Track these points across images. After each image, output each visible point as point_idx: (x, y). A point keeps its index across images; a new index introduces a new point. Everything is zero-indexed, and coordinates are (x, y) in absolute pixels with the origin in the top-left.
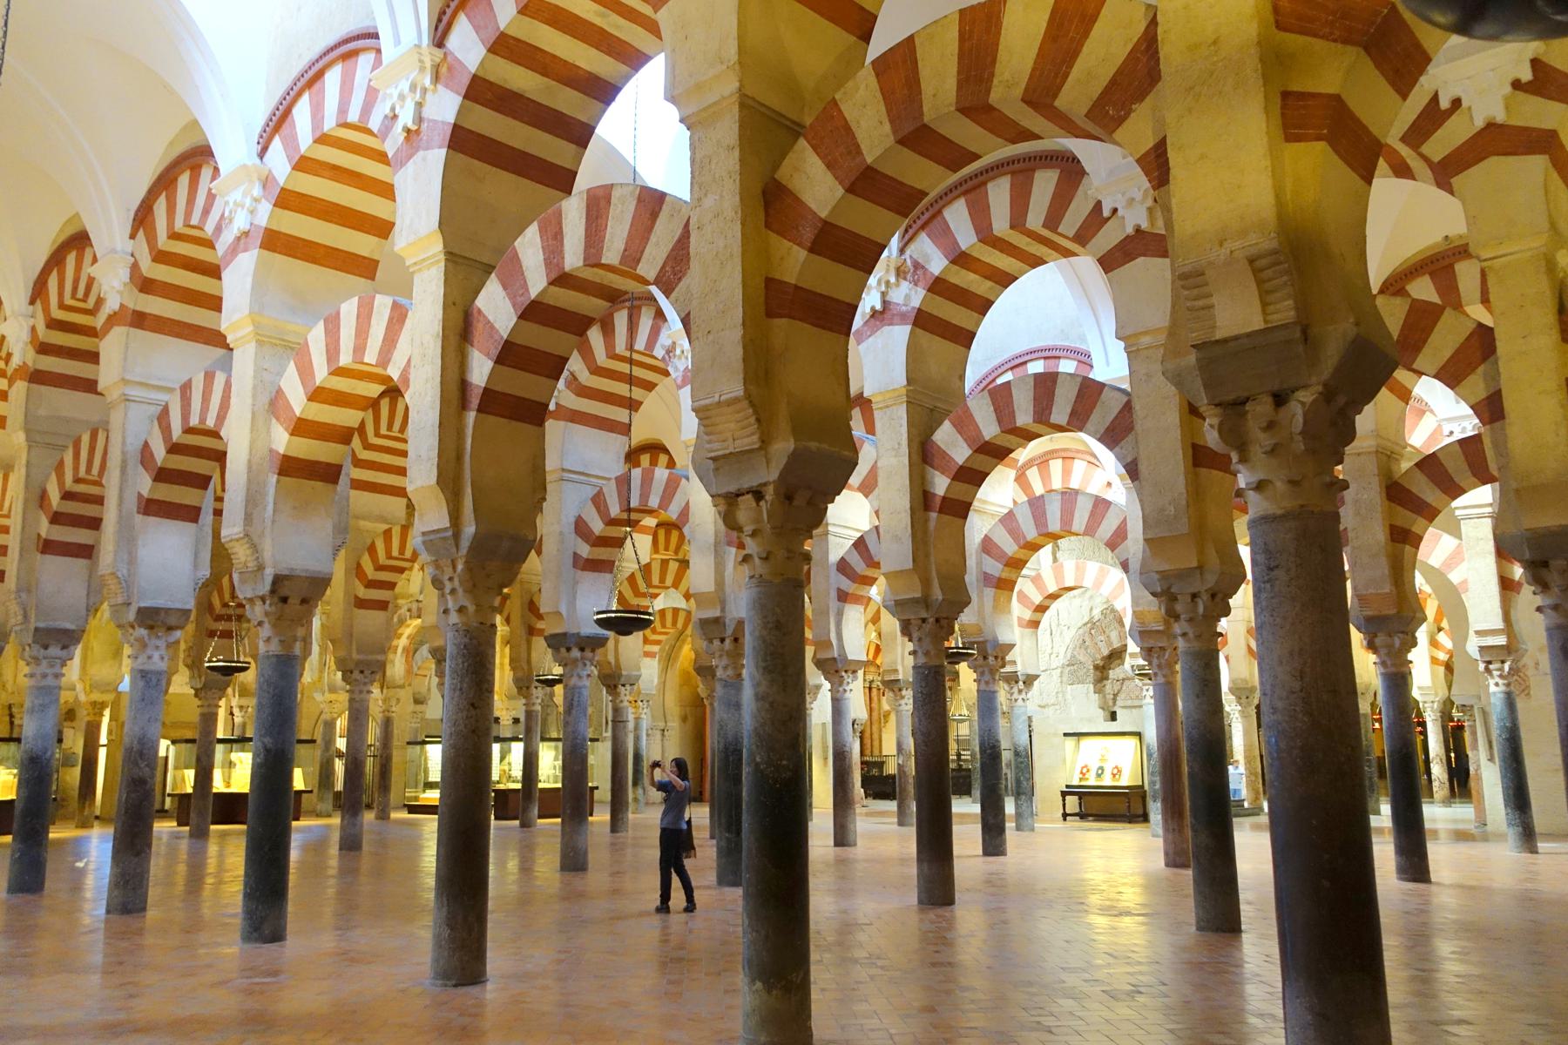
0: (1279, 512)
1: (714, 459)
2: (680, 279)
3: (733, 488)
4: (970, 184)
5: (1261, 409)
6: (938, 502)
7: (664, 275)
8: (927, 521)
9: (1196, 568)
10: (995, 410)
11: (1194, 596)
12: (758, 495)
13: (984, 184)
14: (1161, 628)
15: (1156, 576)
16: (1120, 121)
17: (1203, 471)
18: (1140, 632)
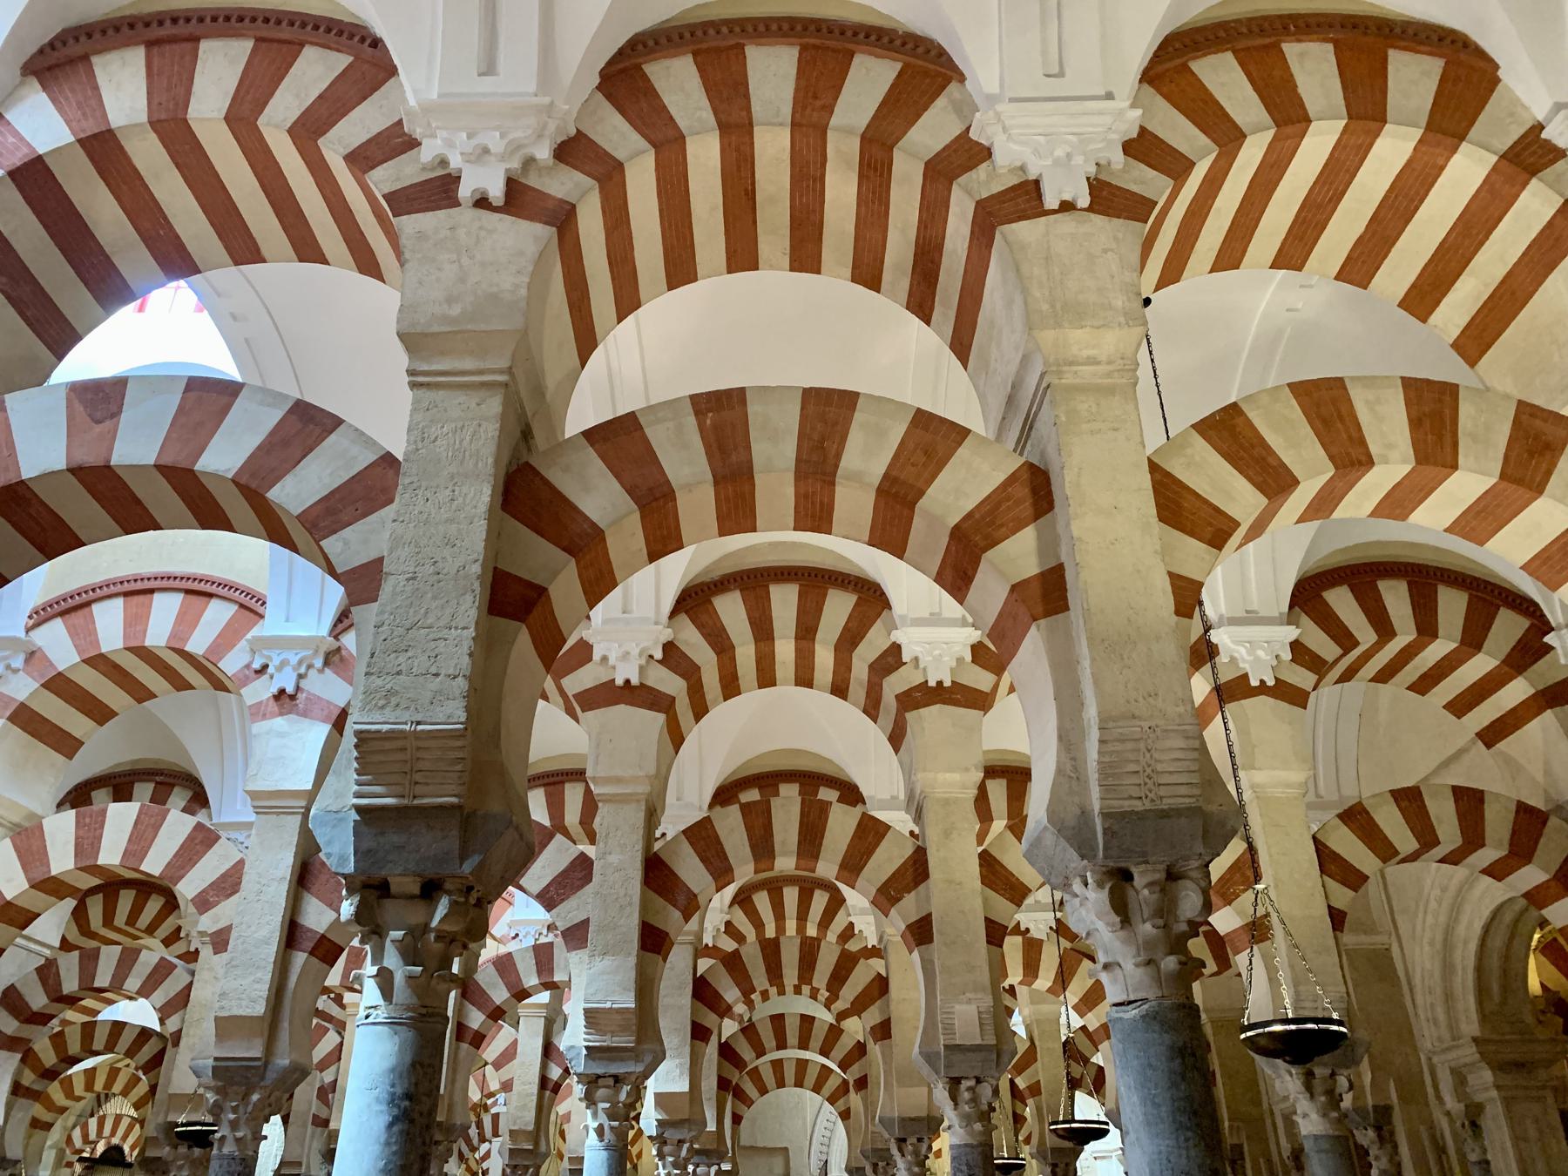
0: (975, 1143)
1: (587, 1048)
2: (563, 900)
3: (600, 1071)
4: (552, 780)
5: (965, 1084)
6: (469, 1037)
7: (548, 893)
8: (457, 1048)
9: (686, 1120)
10: (537, 963)
11: (681, 1142)
12: (618, 1079)
13: (563, 782)
14: (531, 1147)
15: (656, 1123)
16: (899, 900)
17: (698, 1043)
18: (510, 1149)
